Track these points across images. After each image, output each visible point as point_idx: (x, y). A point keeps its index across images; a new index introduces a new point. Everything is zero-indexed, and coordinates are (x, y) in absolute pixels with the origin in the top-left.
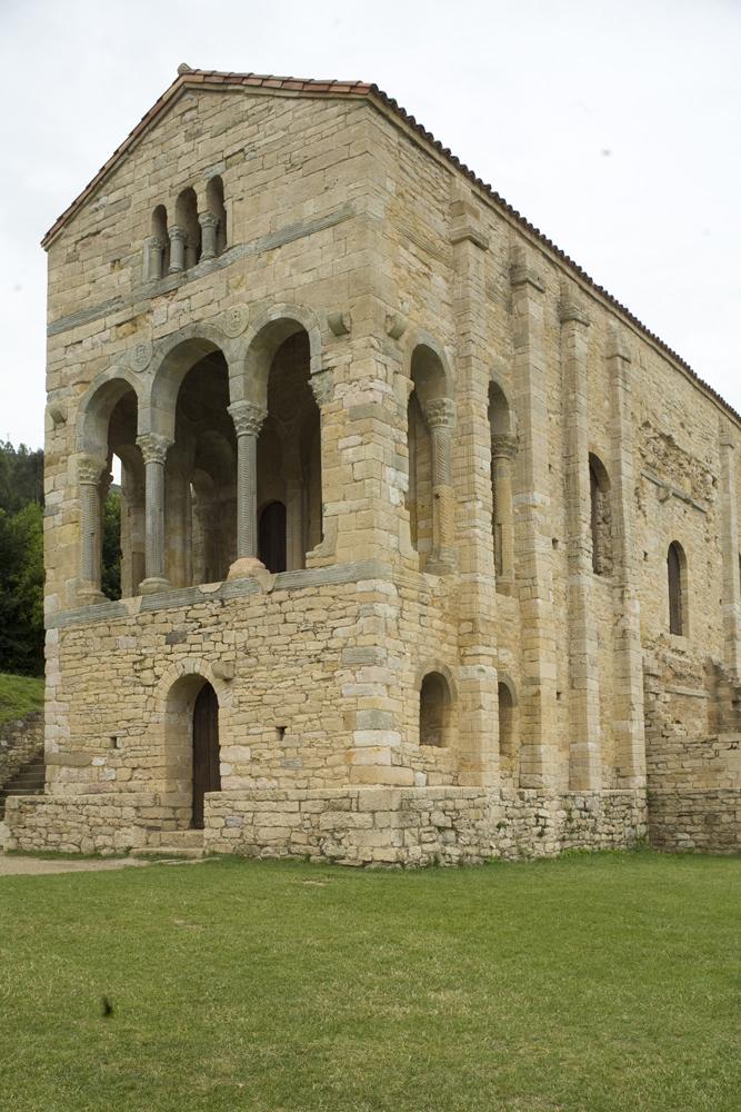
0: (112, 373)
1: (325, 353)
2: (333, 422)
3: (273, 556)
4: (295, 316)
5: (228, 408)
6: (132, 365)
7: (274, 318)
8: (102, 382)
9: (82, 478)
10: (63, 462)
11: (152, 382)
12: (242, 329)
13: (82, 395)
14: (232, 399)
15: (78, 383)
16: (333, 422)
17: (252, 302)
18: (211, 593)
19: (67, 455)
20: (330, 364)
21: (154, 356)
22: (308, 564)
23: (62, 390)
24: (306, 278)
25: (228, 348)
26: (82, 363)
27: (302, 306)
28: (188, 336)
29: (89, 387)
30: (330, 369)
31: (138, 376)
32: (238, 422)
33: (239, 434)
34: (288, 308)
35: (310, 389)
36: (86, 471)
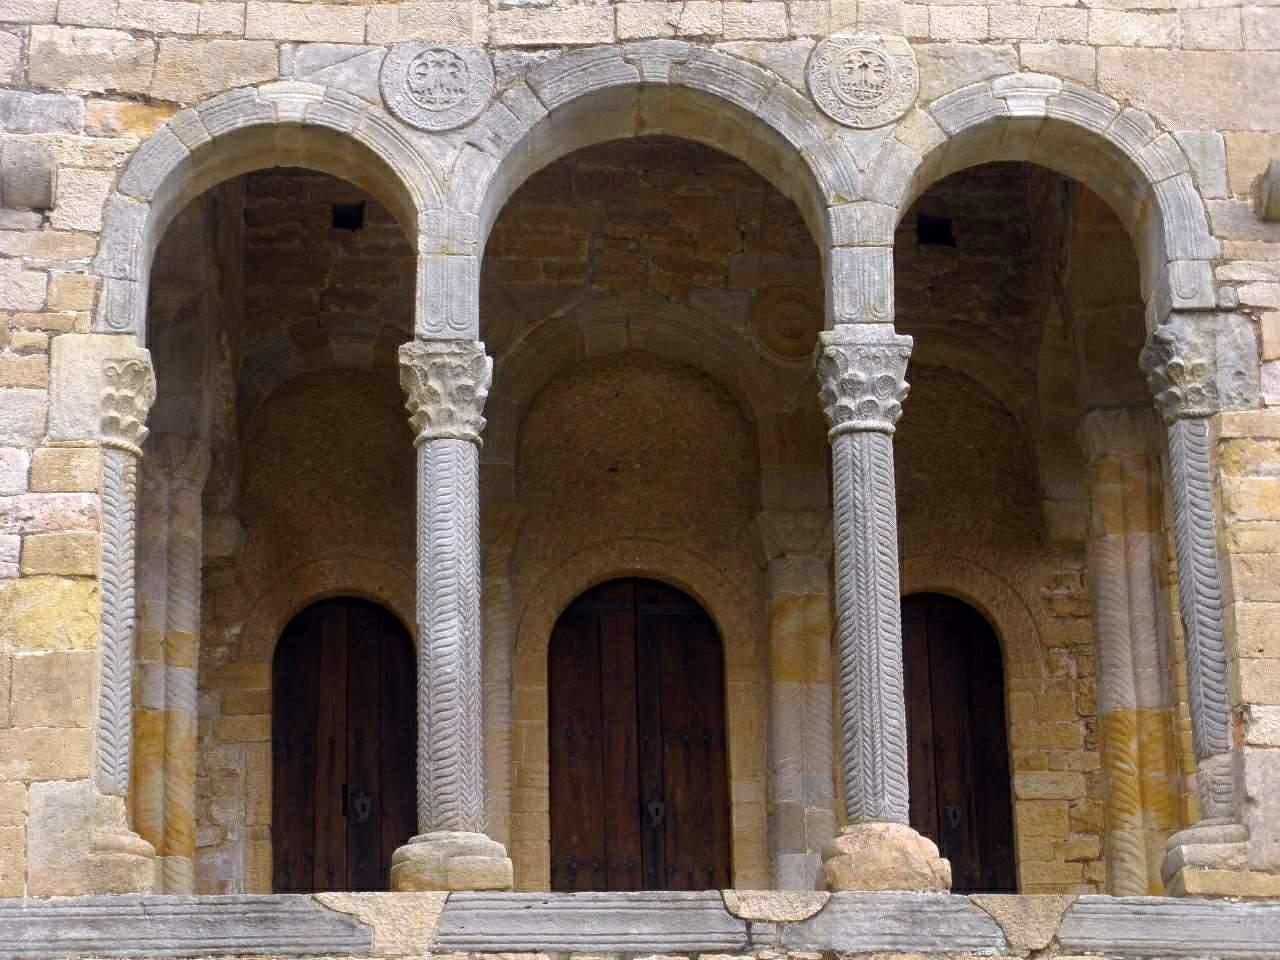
0: (293, 101)
1: (1225, 261)
2: (1266, 465)
3: (977, 833)
4: (1104, 126)
5: (825, 336)
6: (395, 100)
7: (1019, 108)
8: (240, 123)
9: (110, 425)
10: (25, 350)
11: (485, 177)
12: (890, 109)
13: (132, 138)
14: (841, 304)
15: (111, 93)
16: (1266, 465)
17: (928, 40)
18: (780, 925)
19: (53, 332)
20: (1246, 295)
21: (498, 96)
22: (1192, 881)
23: (31, 99)
24: (1135, 29)
25: (830, 152)
26: (138, 33)
27: (1127, 103)
28: (657, 72)
29: (163, 120)
30: (1251, 313)
31: (424, 143)
32: (851, 387)
33: (832, 431)
34: (1072, 97)
35: (1163, 347)
36: (128, 400)
